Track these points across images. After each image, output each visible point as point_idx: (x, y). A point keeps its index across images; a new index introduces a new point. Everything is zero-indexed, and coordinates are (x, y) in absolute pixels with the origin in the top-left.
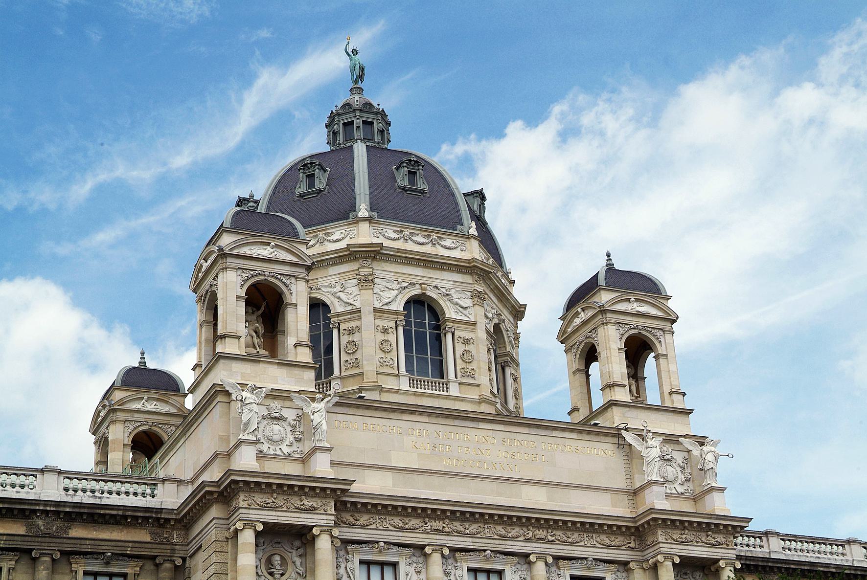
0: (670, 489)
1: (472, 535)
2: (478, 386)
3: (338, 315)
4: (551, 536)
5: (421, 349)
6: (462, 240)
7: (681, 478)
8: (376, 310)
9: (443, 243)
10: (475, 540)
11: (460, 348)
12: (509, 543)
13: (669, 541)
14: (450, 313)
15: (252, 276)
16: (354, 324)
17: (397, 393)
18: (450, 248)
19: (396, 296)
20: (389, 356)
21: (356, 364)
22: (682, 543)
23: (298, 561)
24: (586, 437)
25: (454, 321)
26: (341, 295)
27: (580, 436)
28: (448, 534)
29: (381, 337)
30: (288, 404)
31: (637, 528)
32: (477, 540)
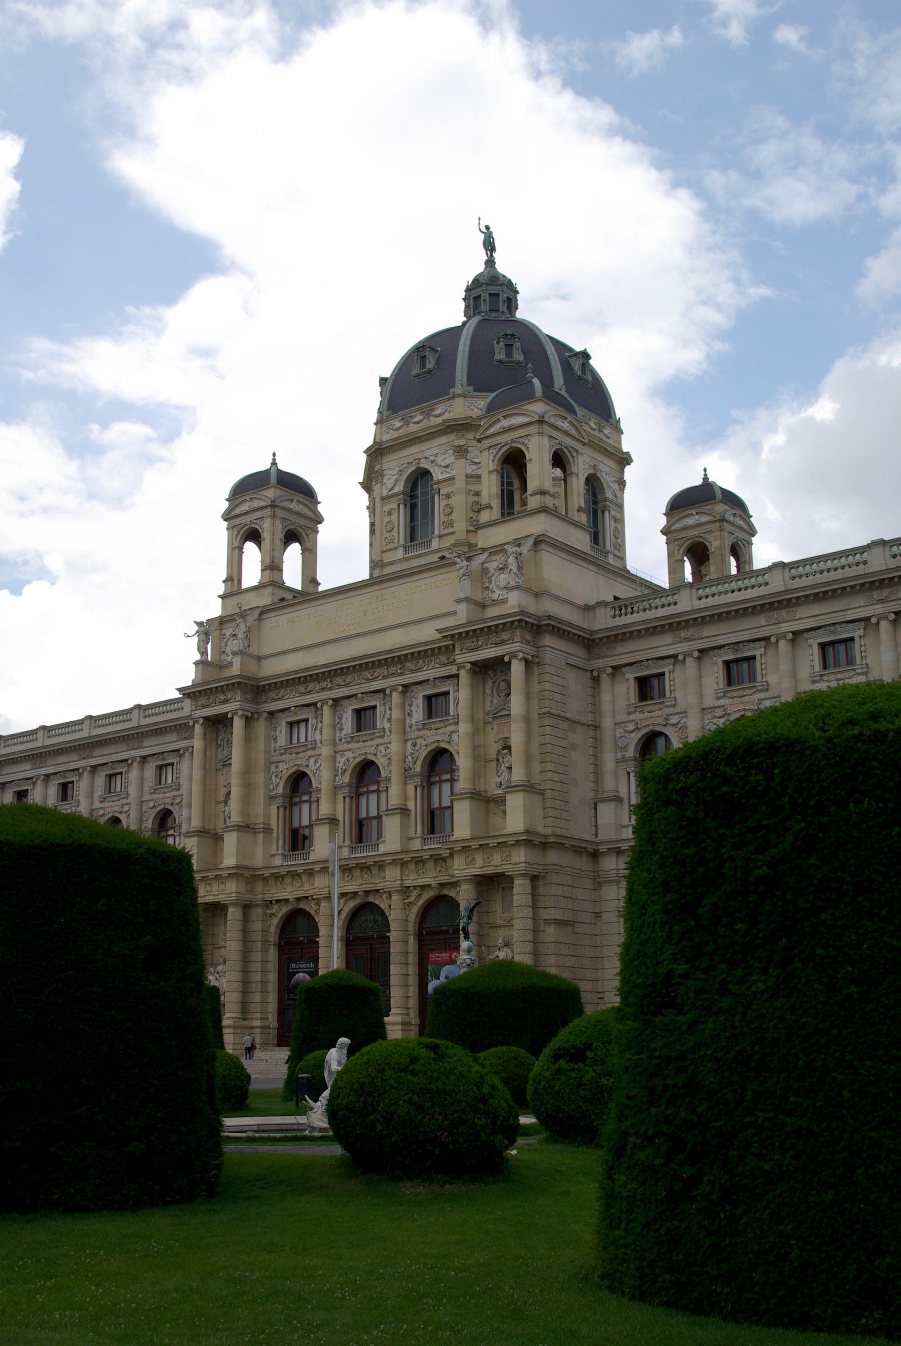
0: (503, 595)
1: (347, 685)
2: (453, 533)
4: (400, 669)
6: (449, 403)
8: (383, 498)
9: (437, 413)
10: (350, 688)
11: (444, 502)
12: (372, 683)
13: (463, 651)
14: (438, 474)
15: (241, 529)
17: (394, 564)
19: (397, 480)
20: (392, 533)
25: (439, 482)
27: (435, 572)
28: (331, 689)
29: (387, 519)
32: (352, 688)
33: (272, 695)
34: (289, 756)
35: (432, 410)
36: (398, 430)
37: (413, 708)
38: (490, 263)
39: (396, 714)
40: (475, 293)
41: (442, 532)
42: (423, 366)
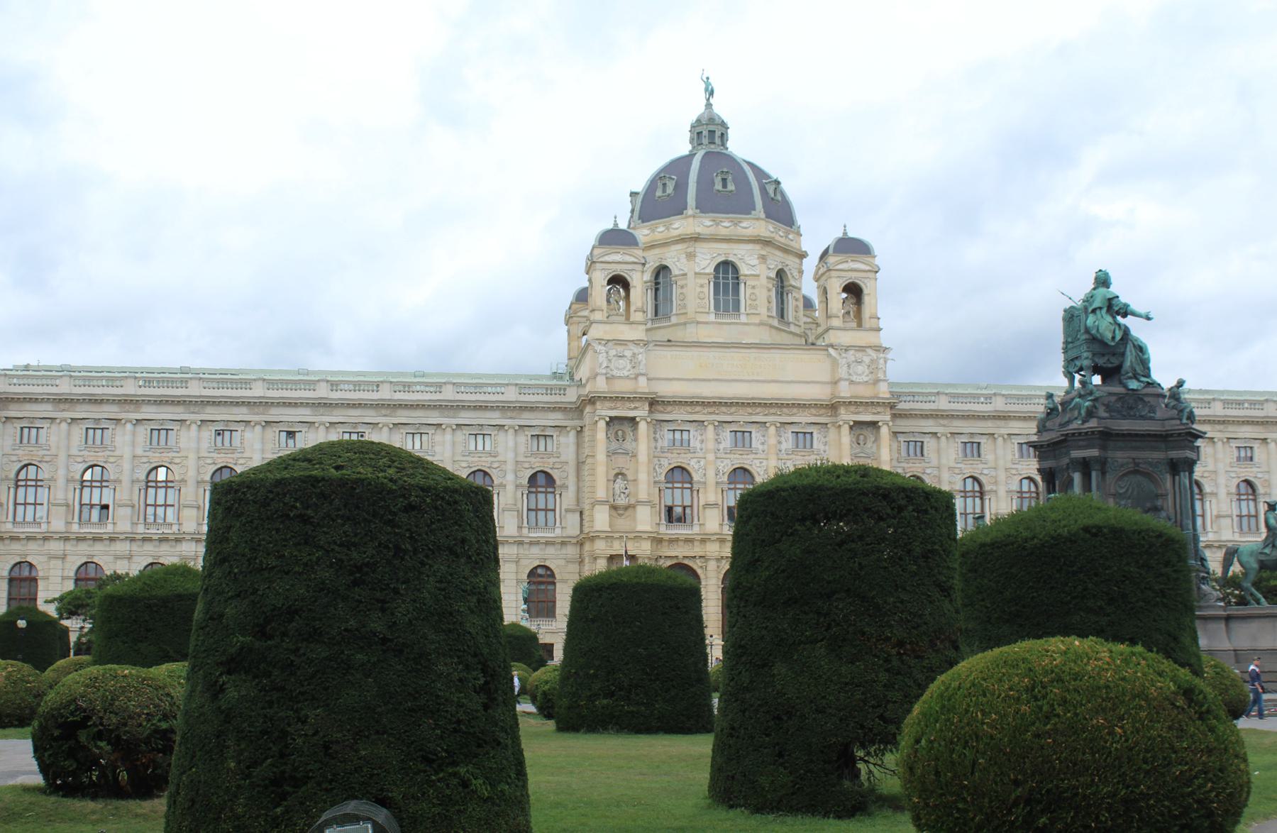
1: (731, 414)
3: (676, 276)
5: (726, 292)
6: (754, 222)
7: (867, 372)
8: (696, 273)
14: (744, 270)
16: (683, 282)
18: (745, 228)
20: (704, 301)
21: (685, 306)
22: (856, 413)
23: (631, 434)
24: (807, 352)
25: (746, 276)
26: (677, 263)
28: (717, 414)
29: (699, 290)
30: (627, 347)
31: (832, 405)
33: (660, 408)
34: (669, 455)
35: (740, 222)
36: (709, 227)
37: (783, 439)
38: (709, 105)
39: (772, 441)
40: (712, 128)
41: (748, 312)
42: (725, 186)
